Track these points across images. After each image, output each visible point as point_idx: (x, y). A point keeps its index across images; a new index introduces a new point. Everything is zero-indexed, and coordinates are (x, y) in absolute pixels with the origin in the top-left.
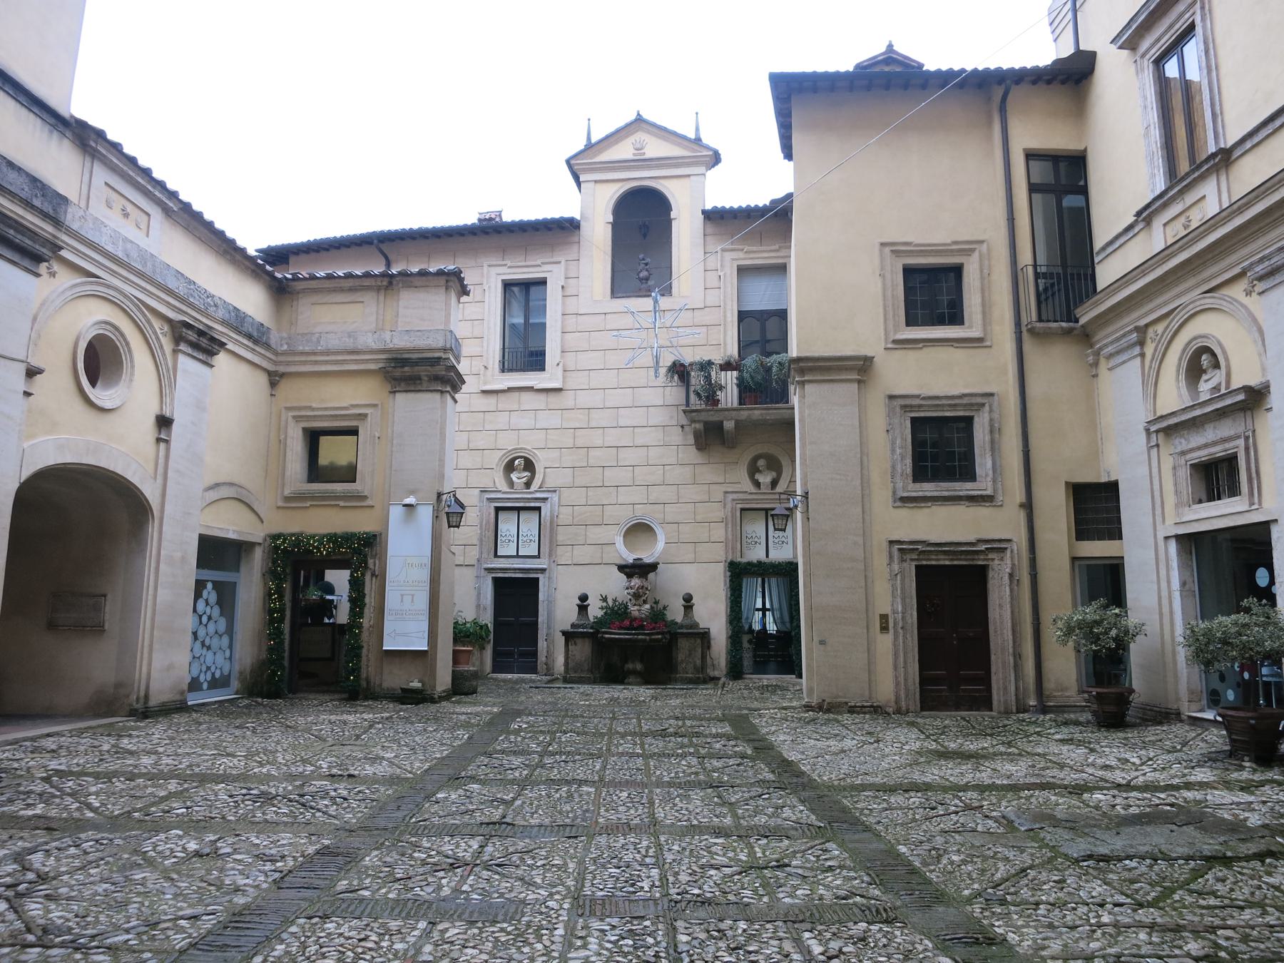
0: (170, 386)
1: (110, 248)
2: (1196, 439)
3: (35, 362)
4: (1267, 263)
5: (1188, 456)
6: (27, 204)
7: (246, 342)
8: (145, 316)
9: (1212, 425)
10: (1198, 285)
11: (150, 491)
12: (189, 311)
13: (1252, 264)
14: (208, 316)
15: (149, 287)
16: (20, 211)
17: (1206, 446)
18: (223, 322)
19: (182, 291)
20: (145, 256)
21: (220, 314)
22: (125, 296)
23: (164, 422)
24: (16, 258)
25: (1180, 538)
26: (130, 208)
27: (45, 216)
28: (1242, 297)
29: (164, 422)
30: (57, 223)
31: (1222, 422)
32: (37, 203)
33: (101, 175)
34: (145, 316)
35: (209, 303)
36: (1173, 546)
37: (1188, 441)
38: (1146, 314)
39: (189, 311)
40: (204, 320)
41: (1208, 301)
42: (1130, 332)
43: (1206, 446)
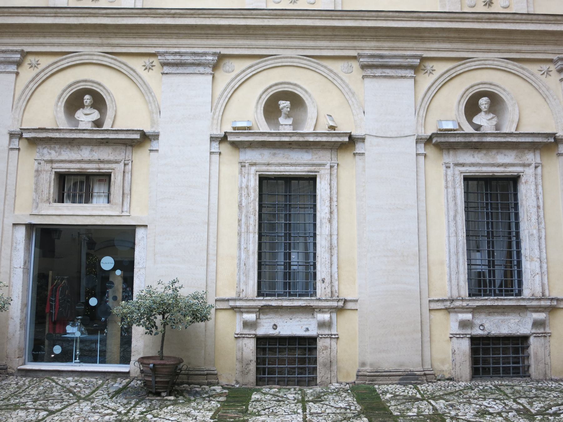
2: (67, 154)
4: (178, 57)
5: (55, 165)
9: (89, 148)
10: (102, 45)
13: (167, 53)
17: (79, 161)
25: (30, 227)
28: (140, 70)
31: (101, 148)
36: (21, 233)
37: (60, 154)
38: (33, 44)
41: (107, 60)
42: (16, 52)
43: (79, 161)
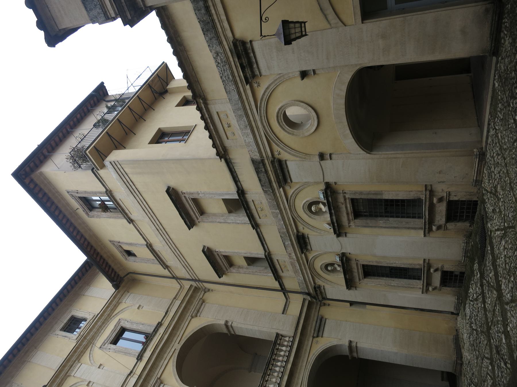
0: (283, 76)
1: (251, 136)
3: (317, 158)
6: (266, 172)
7: (213, 12)
8: (261, 103)
11: (348, 77)
12: (236, 74)
14: (228, 58)
15: (248, 107)
16: (270, 172)
18: (221, 43)
19: (233, 87)
20: (239, 118)
21: (219, 49)
22: (261, 117)
23: (304, 74)
24: (286, 170)
26: (226, 126)
27: (264, 165)
29: (304, 74)
30: (263, 161)
32: (263, 170)
33: (228, 143)
34: (261, 103)
35: (222, 63)
39: (236, 74)
40: (231, 59)
